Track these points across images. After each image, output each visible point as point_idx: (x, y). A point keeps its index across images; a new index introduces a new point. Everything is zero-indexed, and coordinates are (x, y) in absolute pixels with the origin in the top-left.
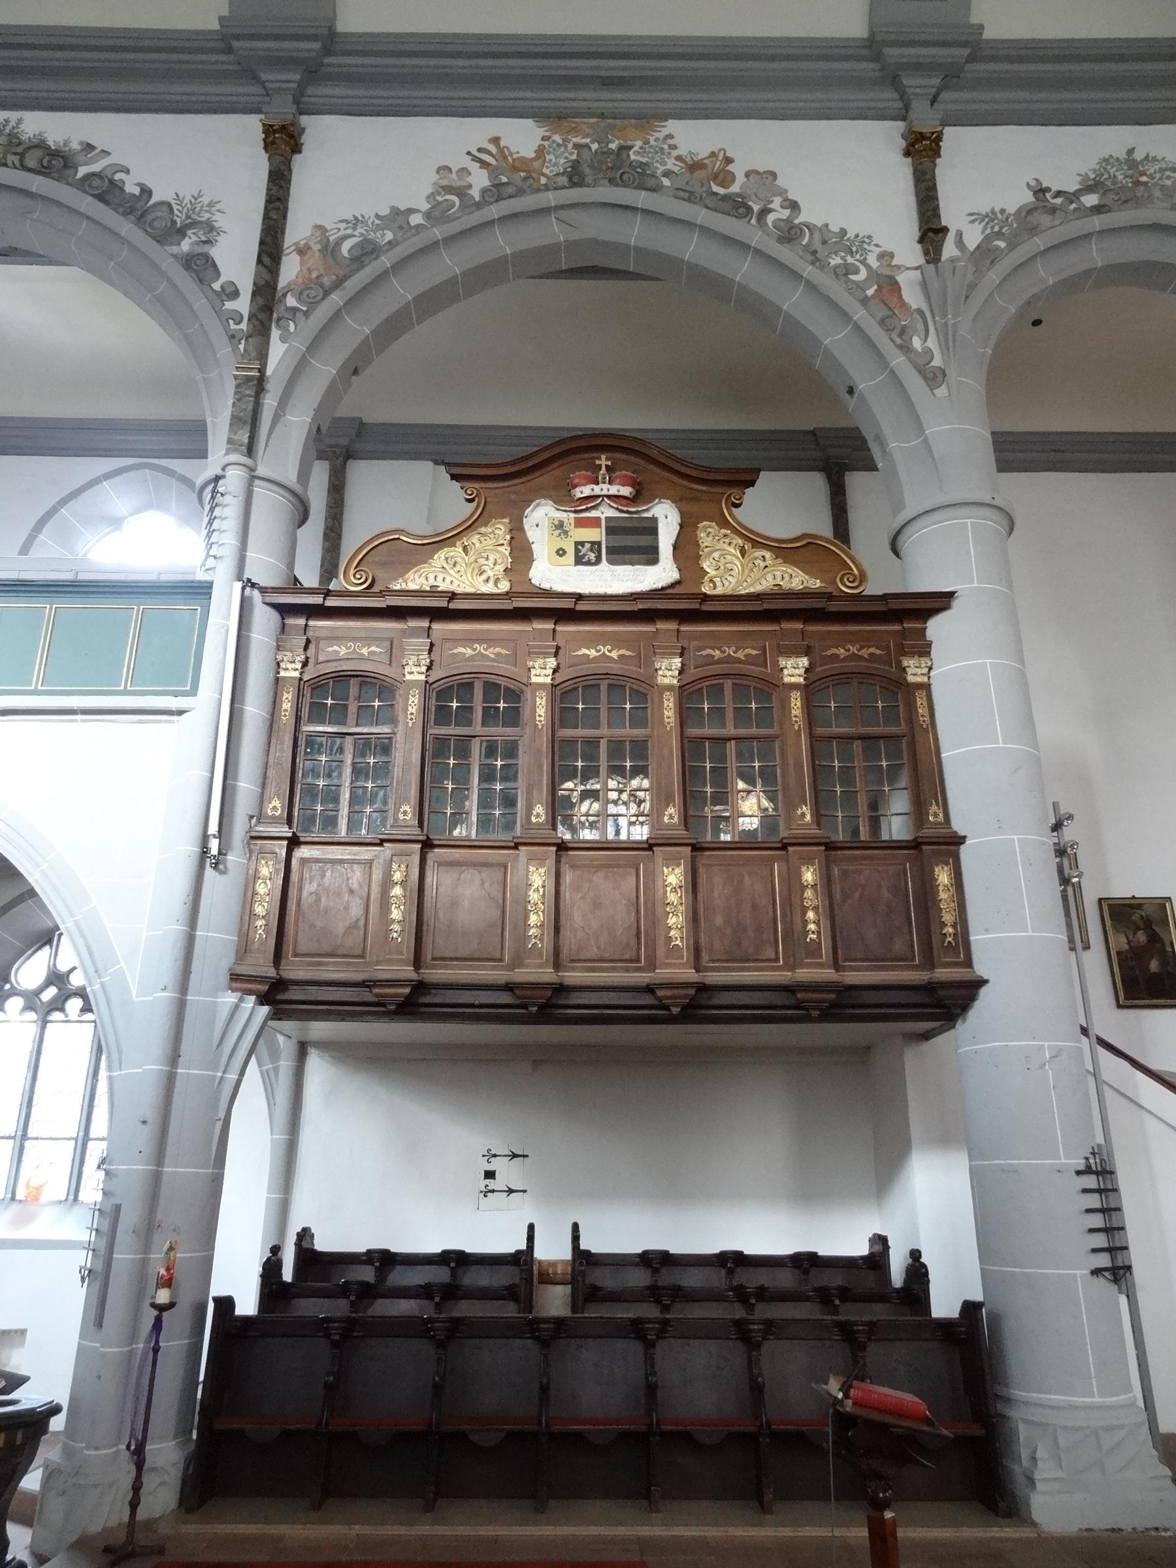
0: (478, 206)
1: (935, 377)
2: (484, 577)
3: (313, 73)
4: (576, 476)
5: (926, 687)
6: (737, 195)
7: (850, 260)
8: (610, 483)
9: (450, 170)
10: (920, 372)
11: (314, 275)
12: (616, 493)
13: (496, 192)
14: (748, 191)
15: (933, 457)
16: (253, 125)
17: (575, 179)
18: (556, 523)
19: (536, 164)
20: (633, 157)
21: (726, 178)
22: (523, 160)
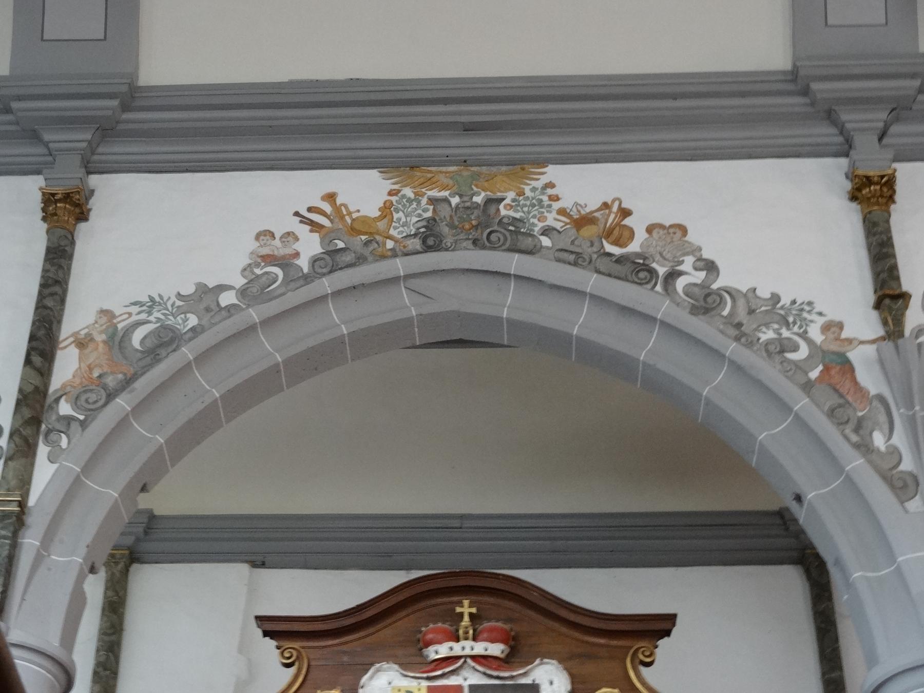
0: (307, 279)
1: (905, 486)
3: (107, 131)
4: (430, 629)
6: (638, 255)
7: (785, 333)
8: (475, 639)
9: (273, 235)
10: (884, 478)
11: (96, 374)
12: (483, 652)
13: (330, 261)
14: (651, 250)
16: (29, 189)
17: (430, 242)
19: (381, 225)
20: (503, 212)
21: (622, 235)
22: (365, 220)
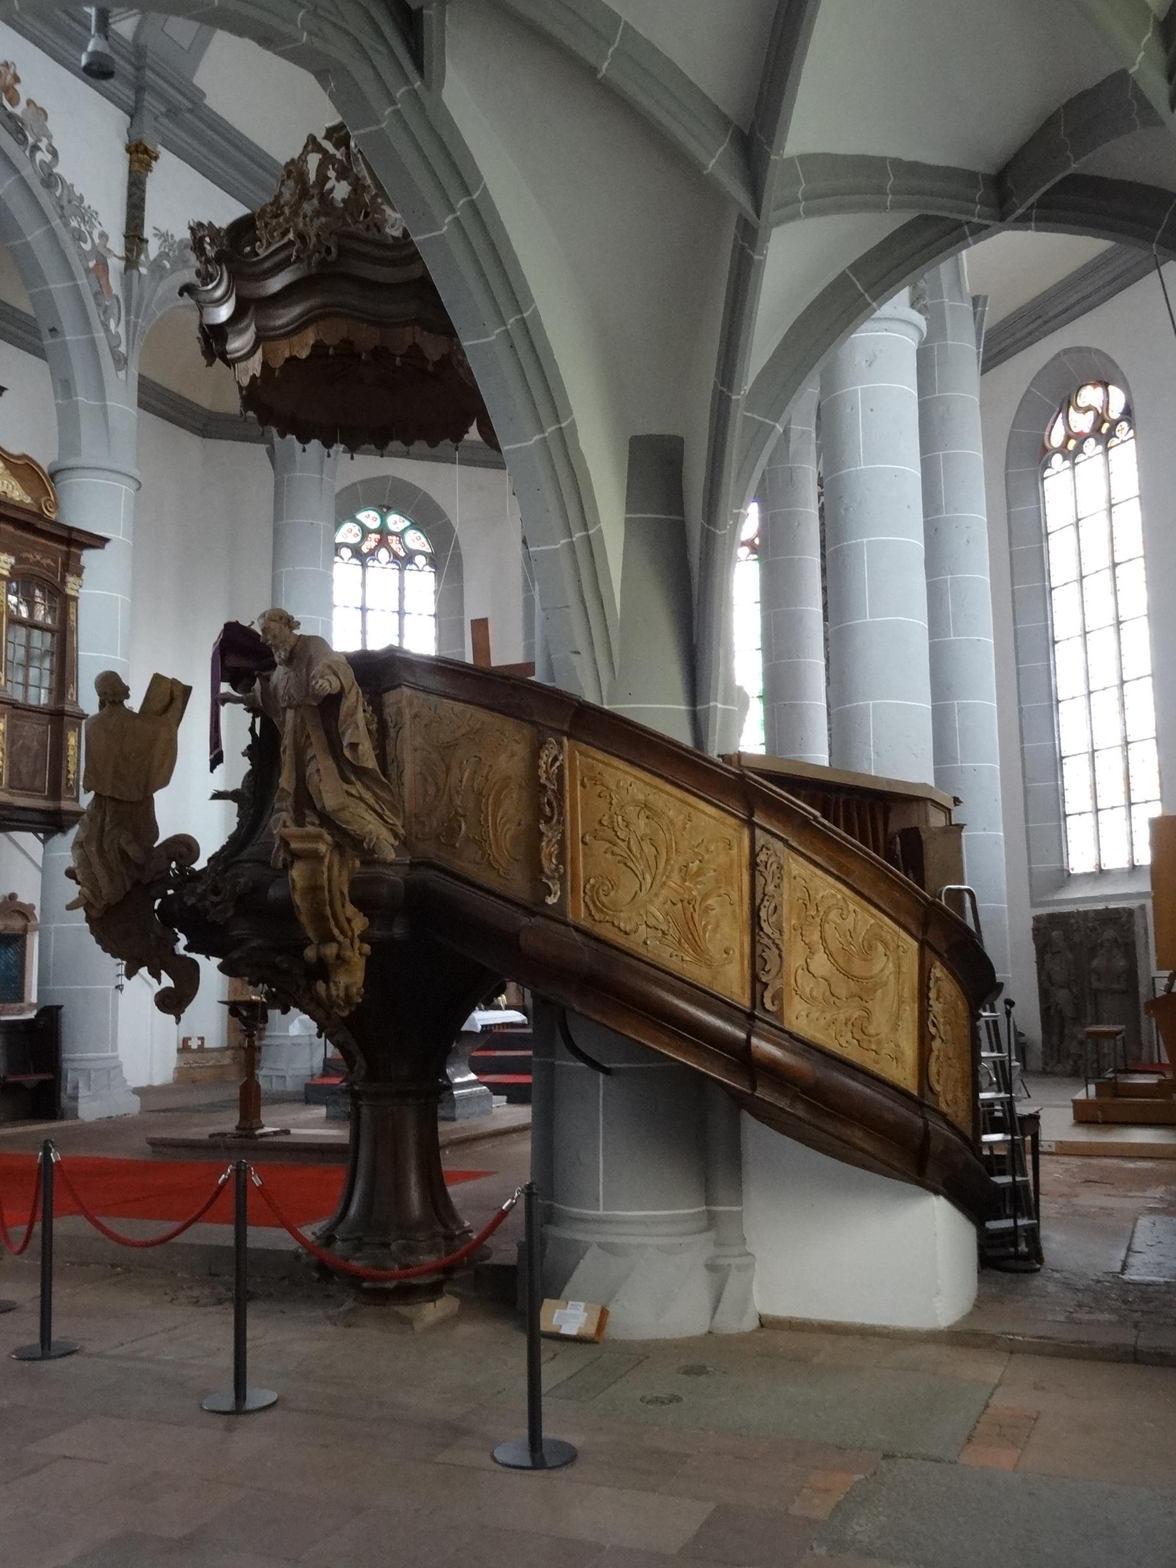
5: (75, 599)
7: (83, 228)
15: (107, 425)
21: (14, 100)
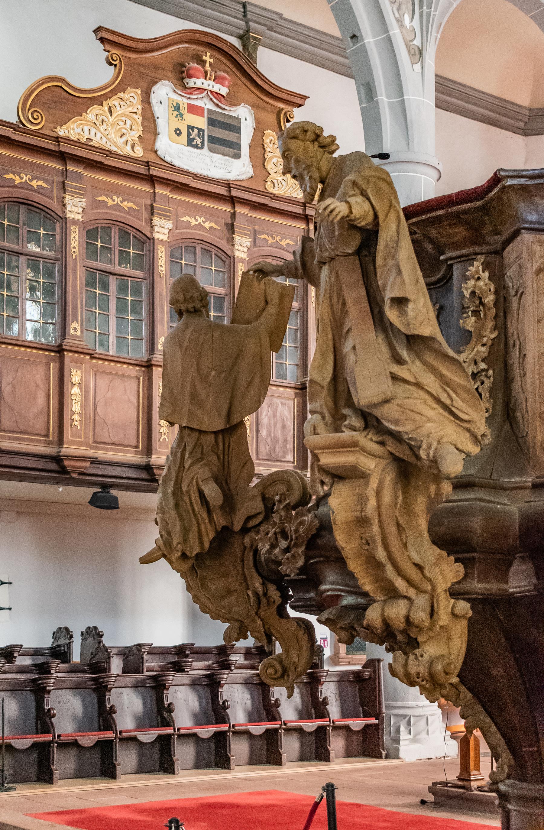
2: (124, 139)
18: (175, 105)
